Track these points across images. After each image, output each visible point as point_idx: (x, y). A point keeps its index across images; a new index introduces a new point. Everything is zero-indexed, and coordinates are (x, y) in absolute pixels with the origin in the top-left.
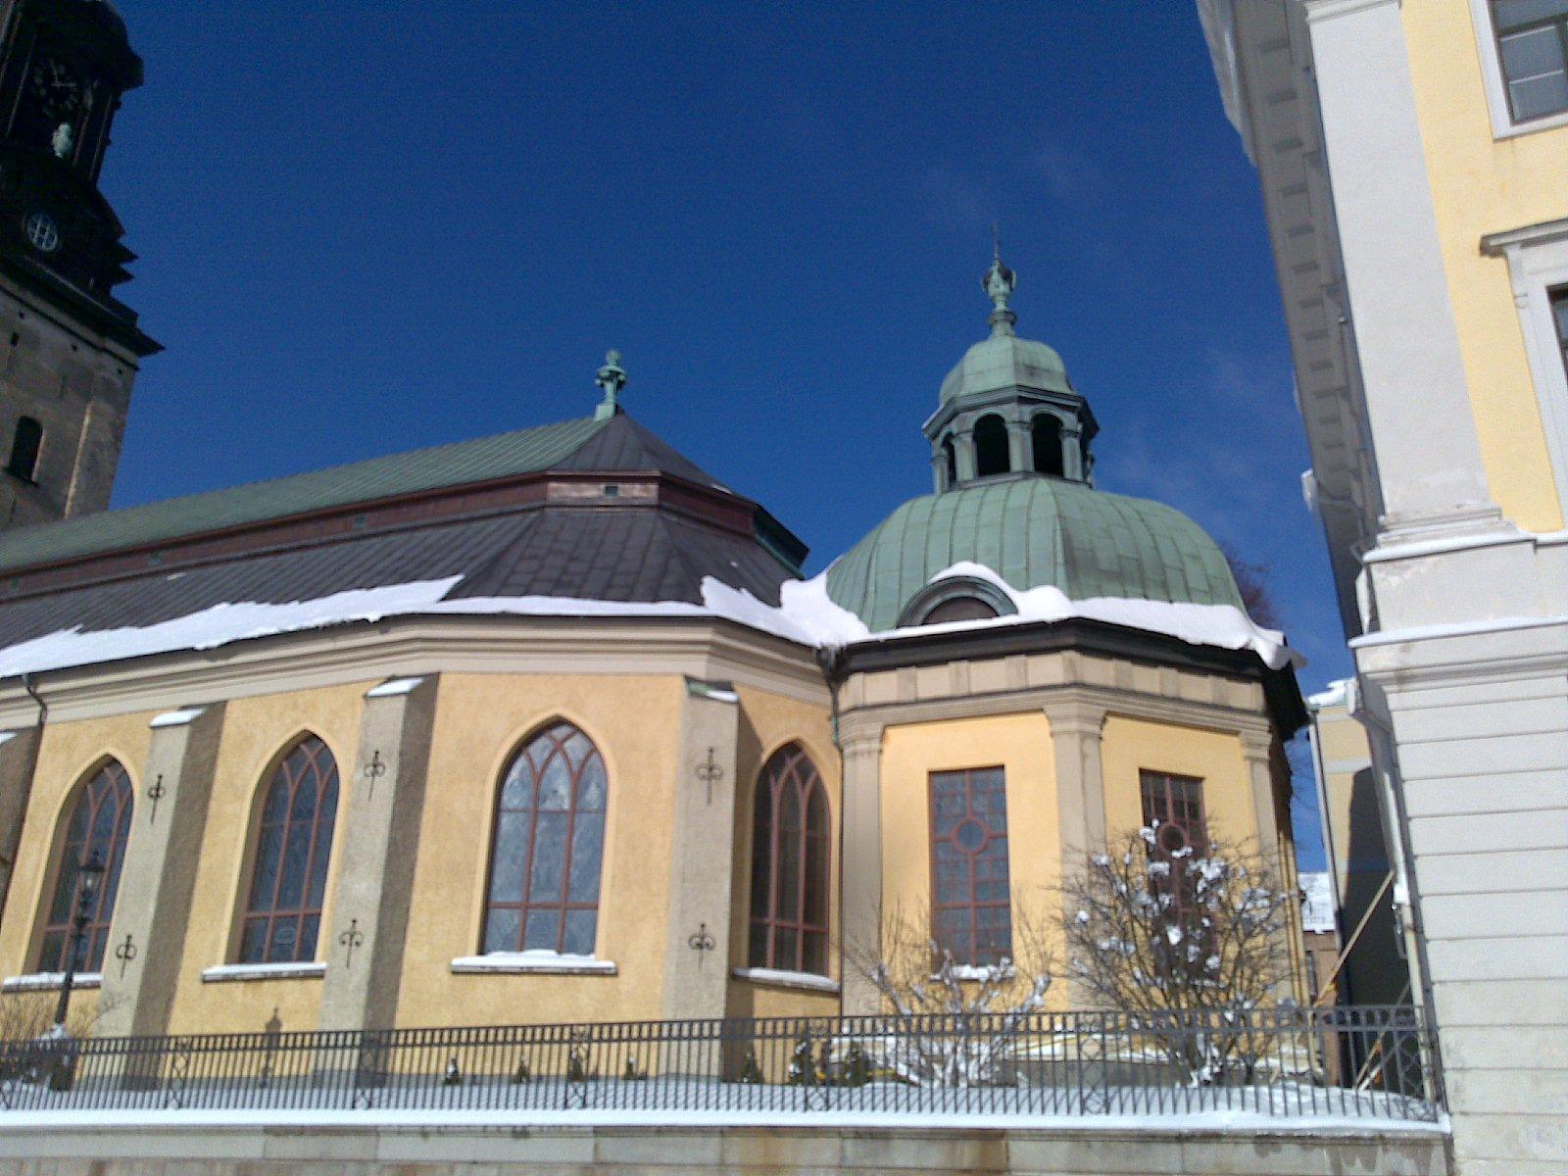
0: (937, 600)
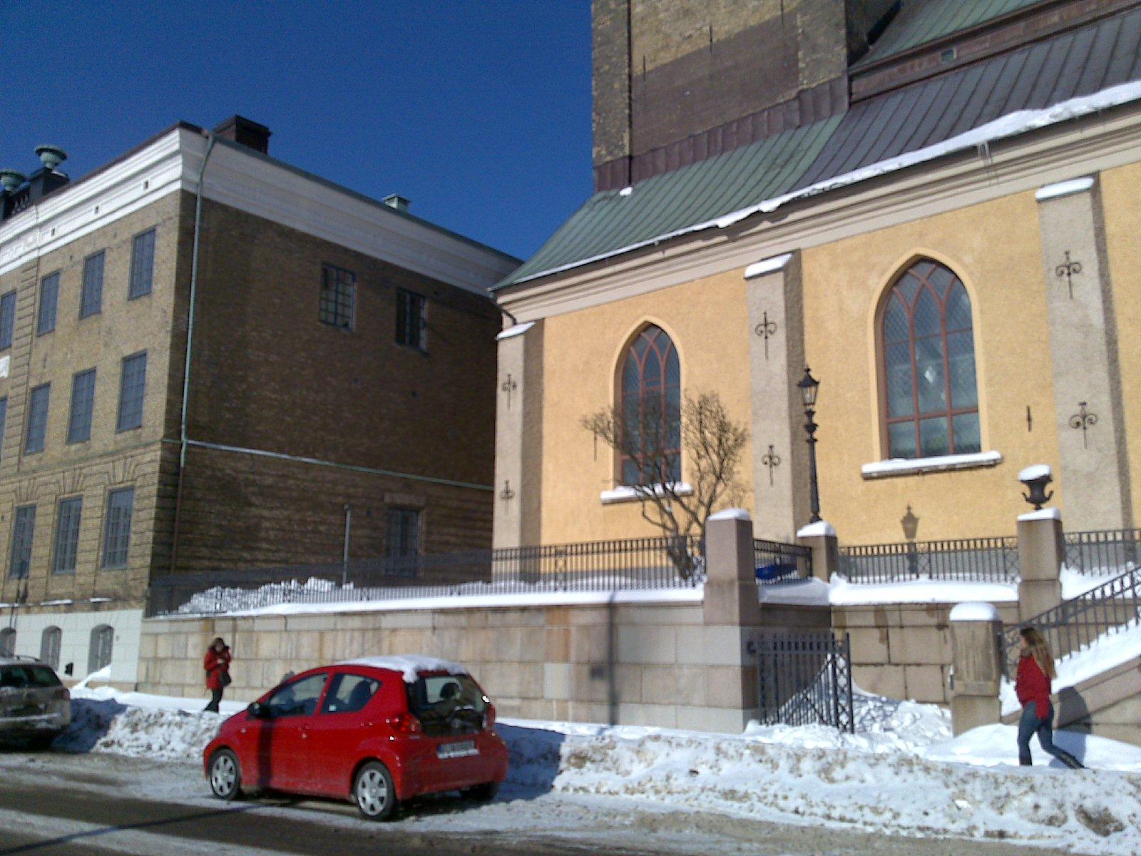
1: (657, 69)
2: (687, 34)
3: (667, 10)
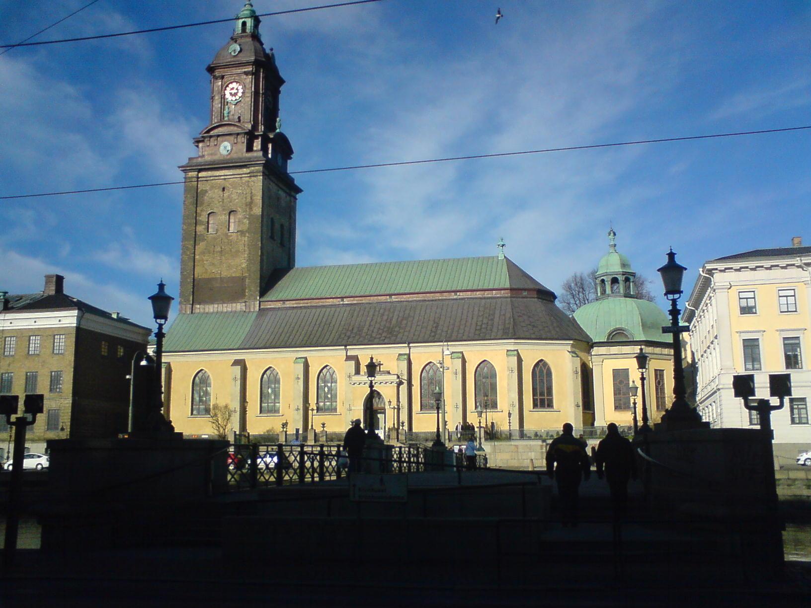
0: (615, 333)
3: (207, 261)
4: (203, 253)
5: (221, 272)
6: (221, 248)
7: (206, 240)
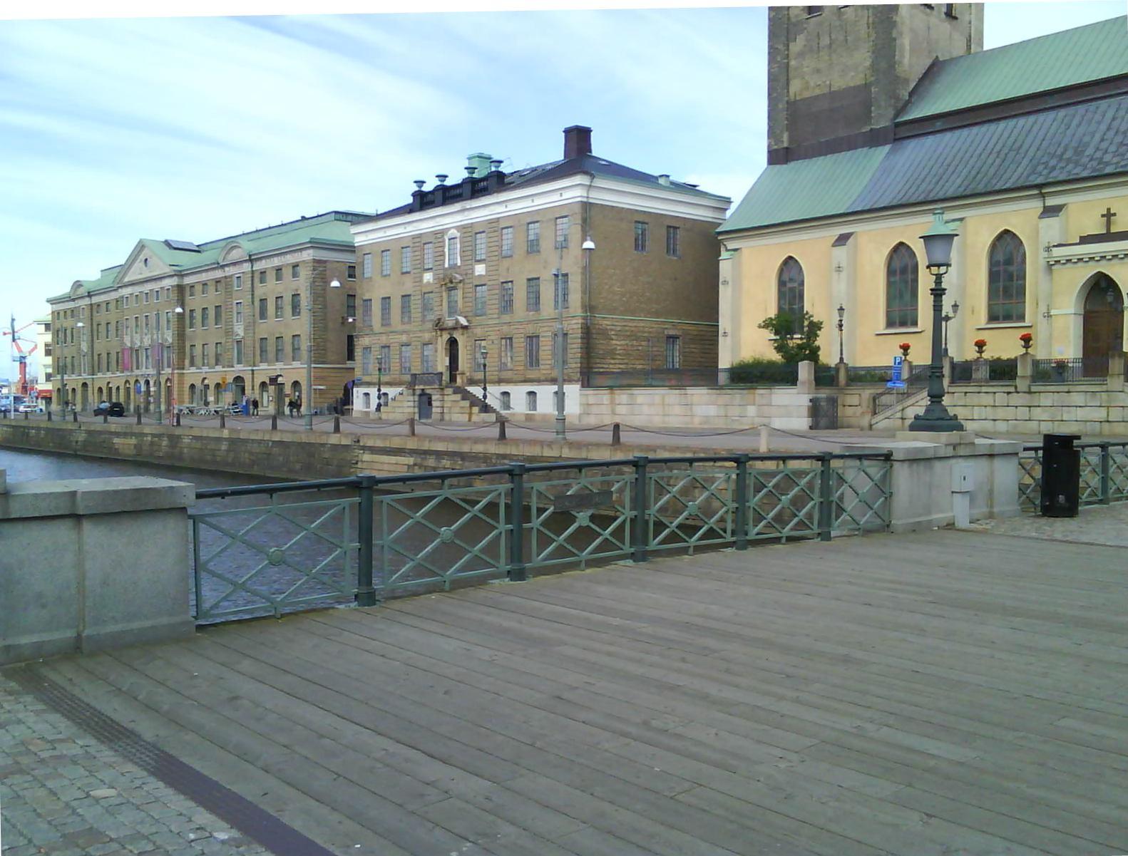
1: (801, 100)
2: (819, 83)
4: (801, 55)
5: (830, 84)
6: (831, 39)
7: (805, 29)
